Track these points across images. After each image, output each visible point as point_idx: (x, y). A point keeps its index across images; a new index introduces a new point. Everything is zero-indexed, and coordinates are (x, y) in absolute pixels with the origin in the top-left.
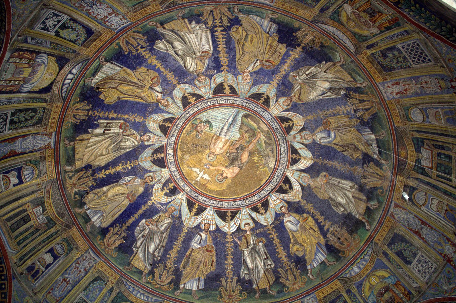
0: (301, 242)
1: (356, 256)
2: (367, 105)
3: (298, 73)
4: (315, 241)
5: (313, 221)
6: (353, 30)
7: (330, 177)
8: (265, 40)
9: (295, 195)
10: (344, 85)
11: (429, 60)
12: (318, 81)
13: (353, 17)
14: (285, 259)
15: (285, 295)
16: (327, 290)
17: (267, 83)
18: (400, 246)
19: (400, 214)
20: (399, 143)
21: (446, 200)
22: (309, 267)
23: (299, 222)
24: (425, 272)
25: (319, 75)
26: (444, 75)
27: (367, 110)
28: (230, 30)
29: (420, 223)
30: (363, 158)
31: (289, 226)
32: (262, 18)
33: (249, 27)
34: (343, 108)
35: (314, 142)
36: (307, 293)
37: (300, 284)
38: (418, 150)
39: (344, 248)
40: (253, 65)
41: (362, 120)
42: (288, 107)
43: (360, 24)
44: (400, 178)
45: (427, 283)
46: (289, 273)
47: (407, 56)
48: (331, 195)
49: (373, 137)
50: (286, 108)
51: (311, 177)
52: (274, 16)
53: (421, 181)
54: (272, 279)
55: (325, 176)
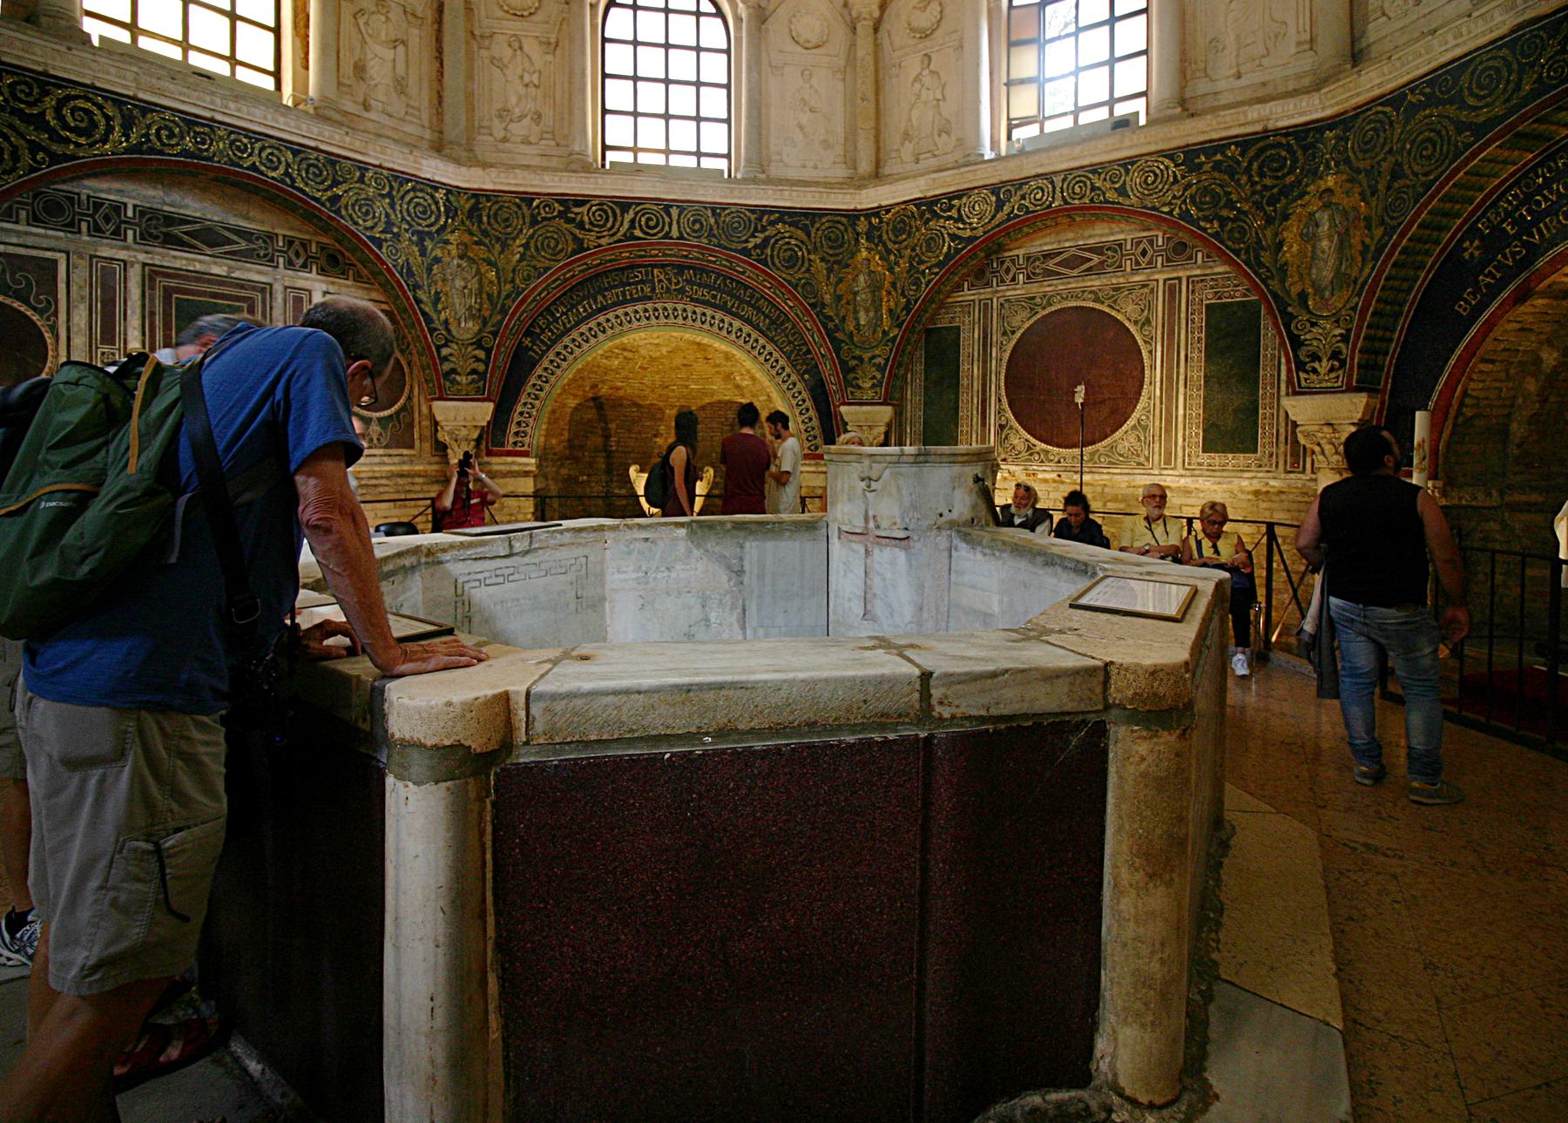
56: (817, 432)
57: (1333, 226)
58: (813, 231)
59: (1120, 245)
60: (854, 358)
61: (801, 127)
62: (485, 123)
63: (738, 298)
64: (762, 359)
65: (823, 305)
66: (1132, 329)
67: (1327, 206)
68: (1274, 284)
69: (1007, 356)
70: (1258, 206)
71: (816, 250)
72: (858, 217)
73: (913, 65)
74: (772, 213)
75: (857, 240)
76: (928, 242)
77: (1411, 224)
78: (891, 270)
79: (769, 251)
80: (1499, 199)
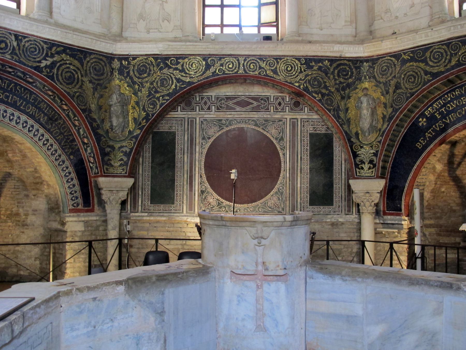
56: (79, 194)
57: (368, 104)
58: (85, 63)
59: (268, 98)
60: (109, 146)
63: (25, 100)
64: (41, 143)
65: (90, 111)
66: (275, 142)
67: (366, 95)
68: (345, 127)
69: (205, 151)
70: (338, 90)
72: (114, 58)
74: (59, 46)
75: (112, 73)
76: (163, 80)
77: (404, 109)
78: (135, 94)
79: (55, 71)
80: (434, 103)
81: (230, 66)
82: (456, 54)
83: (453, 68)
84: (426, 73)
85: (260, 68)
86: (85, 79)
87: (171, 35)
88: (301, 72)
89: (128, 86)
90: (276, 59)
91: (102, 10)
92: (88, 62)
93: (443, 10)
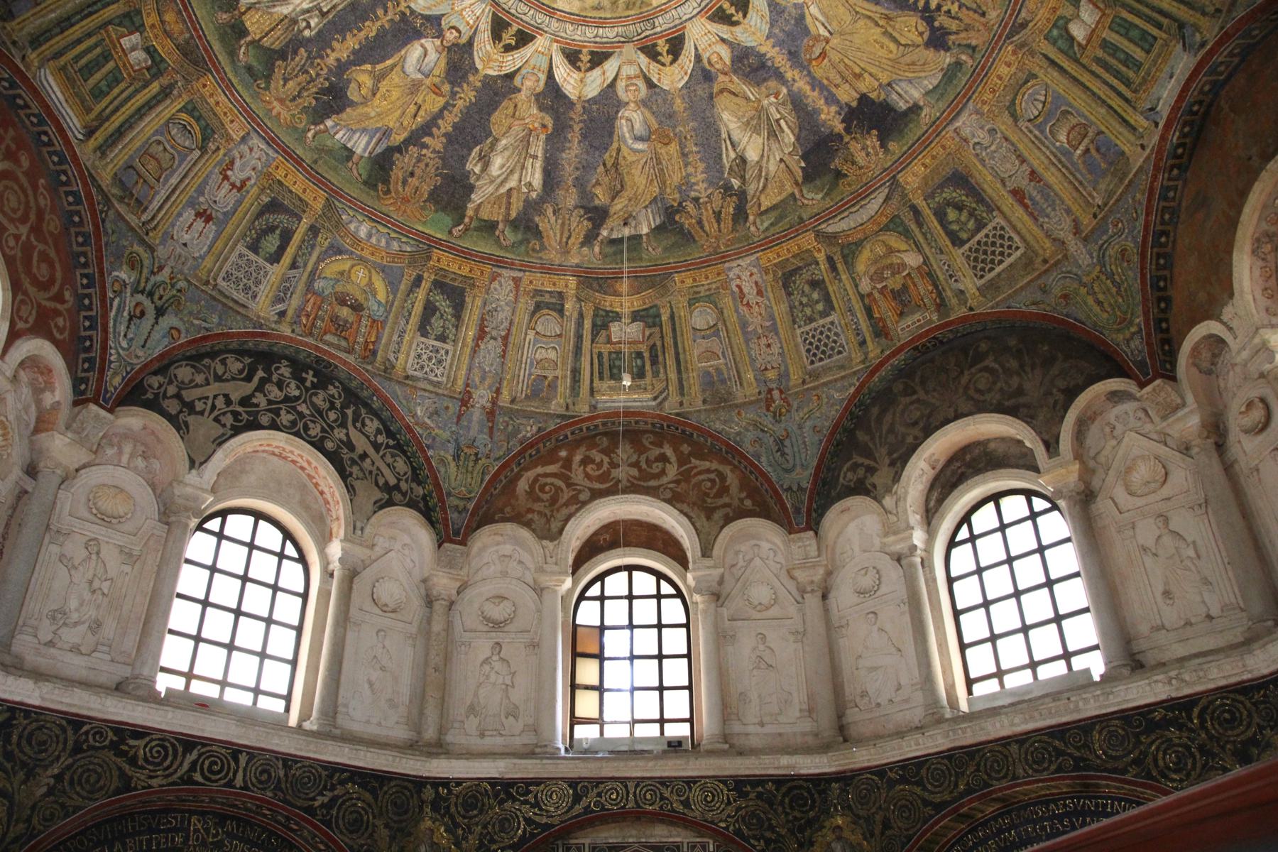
0: (383, 89)
1: (389, 222)
2: (710, 226)
3: (783, 104)
4: (391, 122)
5: (436, 110)
6: (868, 247)
7: (543, 137)
8: (874, 70)
9: (490, 60)
10: (751, 189)
11: (812, 362)
12: (761, 141)
13: (896, 261)
14: (331, 60)
15: (247, 87)
16: (297, 183)
17: (770, 32)
18: (443, 304)
19: (502, 291)
20: (642, 280)
21: (562, 373)
22: (329, 123)
23: (427, 76)
24: (422, 367)
25: (775, 146)
26: (788, 380)
27: (700, 222)
28: (923, 18)
29: (503, 333)
30: (596, 208)
31: (414, 53)
32: (928, 93)
33: (915, 57)
34: (701, 177)
35: (620, 104)
36: (272, 139)
37: (285, 114)
38: (636, 316)
39: (397, 192)
40: (821, 18)
41: (678, 211)
42: (705, 61)
43: (879, 265)
44: (573, 282)
45: (407, 377)
46: (302, 78)
47: (814, 325)
48: (504, 142)
49: (645, 230)
50: (705, 56)
51: (538, 96)
52: (926, 115)
53: (580, 324)
54: (274, 41)
55: (544, 126)
58: (381, 794)
59: (678, 847)
61: (371, 684)
62: (33, 622)
67: (839, 838)
70: (791, 831)
71: (381, 814)
73: (483, 647)
74: (344, 771)
79: (334, 812)
81: (614, 796)
82: (963, 774)
83: (962, 795)
84: (926, 803)
85: (662, 798)
86: (379, 823)
87: (518, 741)
88: (729, 803)
89: (446, 831)
90: (688, 783)
91: (411, 702)
92: (385, 793)
93: (936, 701)
